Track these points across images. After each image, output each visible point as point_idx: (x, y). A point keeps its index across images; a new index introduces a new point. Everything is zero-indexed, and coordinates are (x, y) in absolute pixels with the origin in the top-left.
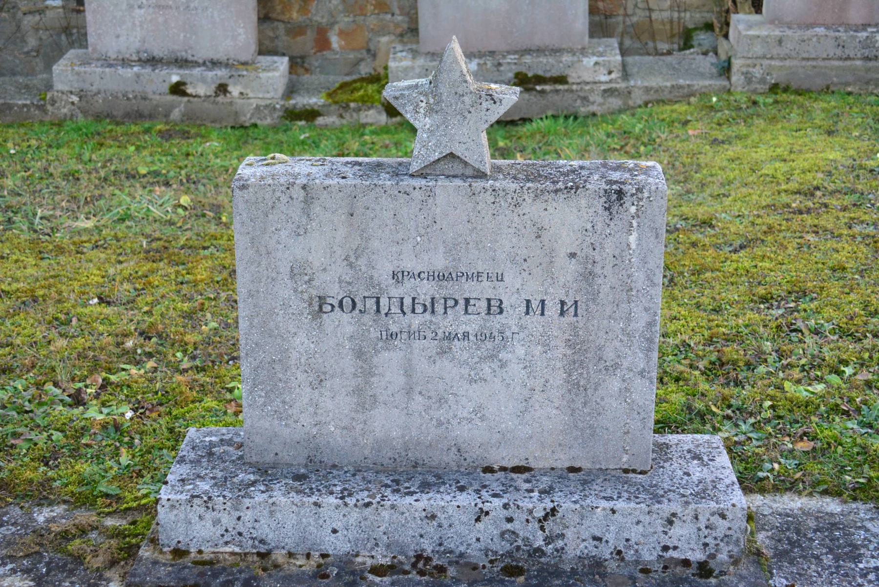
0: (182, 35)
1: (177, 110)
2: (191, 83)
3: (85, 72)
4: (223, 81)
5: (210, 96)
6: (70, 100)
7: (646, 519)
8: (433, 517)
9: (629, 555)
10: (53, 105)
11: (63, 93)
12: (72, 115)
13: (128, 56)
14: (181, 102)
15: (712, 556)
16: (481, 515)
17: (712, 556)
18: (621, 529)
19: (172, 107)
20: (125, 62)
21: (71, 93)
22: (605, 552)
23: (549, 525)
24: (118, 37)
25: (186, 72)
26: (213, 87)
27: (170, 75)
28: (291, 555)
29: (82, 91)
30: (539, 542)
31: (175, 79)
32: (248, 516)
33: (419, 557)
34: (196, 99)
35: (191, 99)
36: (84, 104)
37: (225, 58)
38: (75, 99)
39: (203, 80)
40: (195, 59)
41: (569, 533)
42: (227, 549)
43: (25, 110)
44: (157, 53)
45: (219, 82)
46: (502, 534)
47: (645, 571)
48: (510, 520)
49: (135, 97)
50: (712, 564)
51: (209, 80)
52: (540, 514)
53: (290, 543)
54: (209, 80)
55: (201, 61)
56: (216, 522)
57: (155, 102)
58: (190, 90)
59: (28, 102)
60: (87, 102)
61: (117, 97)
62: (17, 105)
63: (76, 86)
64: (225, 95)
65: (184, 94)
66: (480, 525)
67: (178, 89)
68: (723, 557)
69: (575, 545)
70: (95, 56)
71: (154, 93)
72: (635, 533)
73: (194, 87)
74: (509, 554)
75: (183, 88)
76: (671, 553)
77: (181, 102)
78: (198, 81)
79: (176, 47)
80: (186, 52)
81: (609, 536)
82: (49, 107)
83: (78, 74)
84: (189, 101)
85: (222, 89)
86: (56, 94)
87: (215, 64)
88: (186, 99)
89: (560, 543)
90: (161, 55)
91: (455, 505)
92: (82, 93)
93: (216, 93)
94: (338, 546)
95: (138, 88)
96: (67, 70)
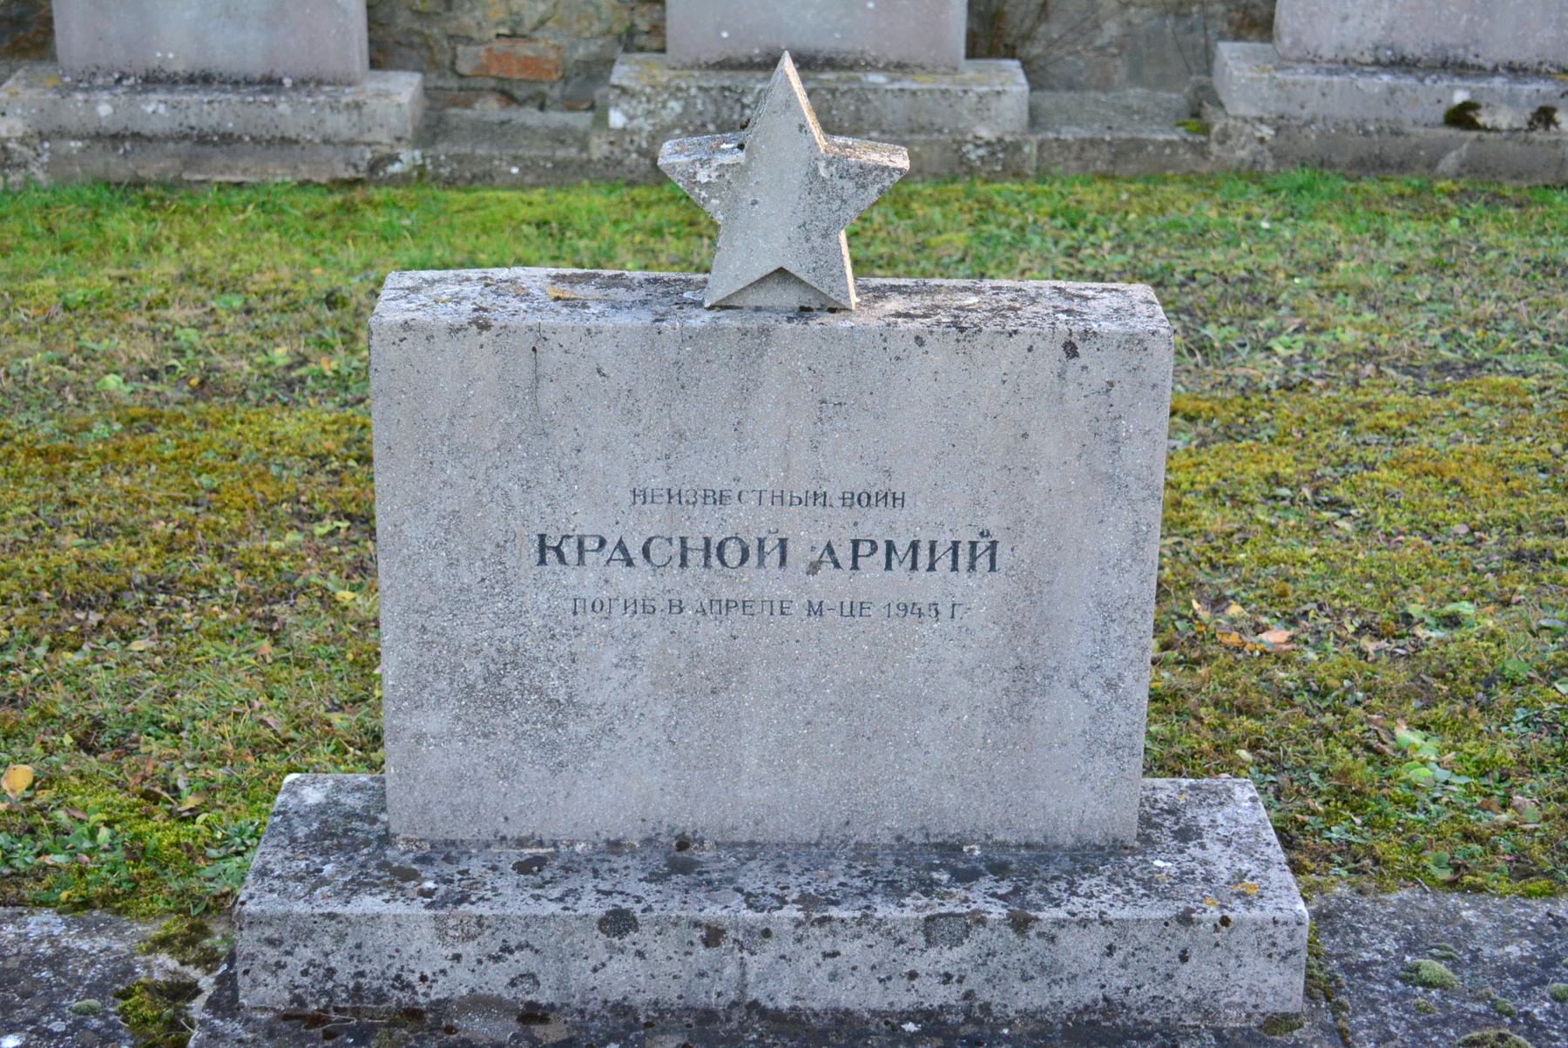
0: (1465, 17)
1: (1453, 154)
2: (1488, 105)
3: (1294, 84)
4: (1547, 103)
5: (1518, 130)
6: (1258, 134)
10: (1222, 143)
11: (1245, 121)
12: (1255, 162)
13: (1355, 55)
14: (1463, 141)
19: (1445, 148)
20: (1349, 65)
21: (1261, 120)
24: (1345, 19)
25: (1483, 85)
26: (1527, 113)
27: (1452, 89)
29: (1282, 117)
31: (1460, 97)
34: (1492, 135)
35: (1484, 135)
36: (1282, 141)
37: (1537, 60)
38: (1267, 132)
39: (1512, 100)
40: (1480, 61)
43: (1168, 151)
44: (1411, 49)
45: (1540, 103)
49: (1380, 131)
51: (1523, 99)
54: (1523, 99)
55: (1489, 66)
57: (1414, 140)
58: (1483, 119)
59: (1175, 137)
60: (1288, 138)
61: (1345, 130)
62: (1153, 142)
63: (1274, 108)
64: (1547, 128)
65: (1472, 125)
67: (1461, 117)
70: (1297, 53)
71: (1415, 123)
73: (1493, 113)
75: (1472, 114)
77: (1463, 141)
78: (1502, 101)
79: (1448, 40)
80: (1466, 48)
82: (1214, 148)
83: (1281, 86)
84: (1479, 139)
85: (1545, 116)
86: (1232, 122)
87: (1515, 71)
88: (1473, 134)
90: (1418, 53)
92: (1281, 122)
93: (1530, 123)
95: (1387, 113)
96: (1262, 79)
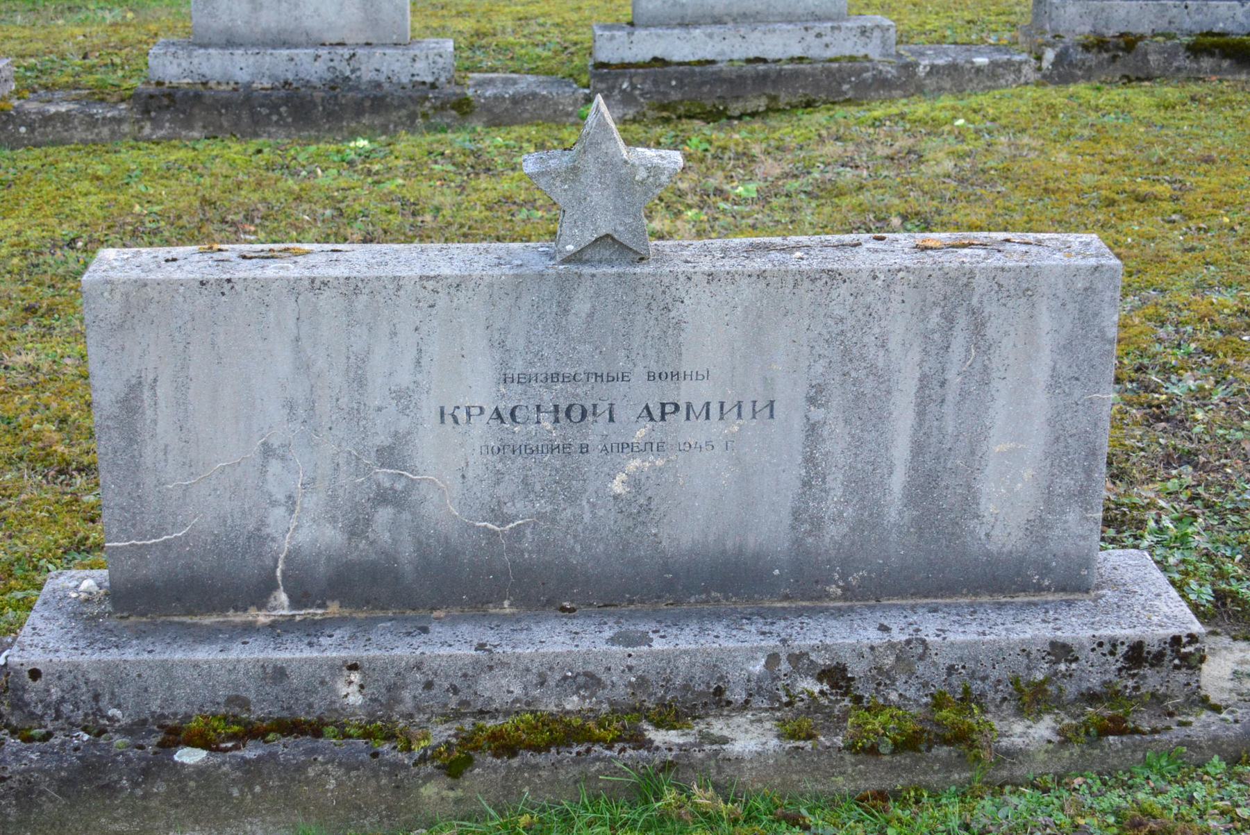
7: (401, 58)
8: (292, 60)
9: (395, 79)
15: (437, 79)
16: (317, 57)
17: (437, 79)
18: (389, 64)
22: (382, 78)
23: (352, 62)
28: (219, 83)
30: (348, 73)
32: (196, 61)
33: (286, 83)
41: (363, 68)
42: (186, 81)
46: (328, 69)
47: (403, 88)
48: (332, 60)
50: (437, 84)
52: (347, 56)
53: (218, 76)
56: (179, 65)
66: (317, 64)
68: (442, 79)
69: (367, 74)
72: (396, 67)
74: (332, 80)
76: (416, 78)
81: (384, 69)
89: (358, 73)
91: (304, 54)
94: (243, 77)
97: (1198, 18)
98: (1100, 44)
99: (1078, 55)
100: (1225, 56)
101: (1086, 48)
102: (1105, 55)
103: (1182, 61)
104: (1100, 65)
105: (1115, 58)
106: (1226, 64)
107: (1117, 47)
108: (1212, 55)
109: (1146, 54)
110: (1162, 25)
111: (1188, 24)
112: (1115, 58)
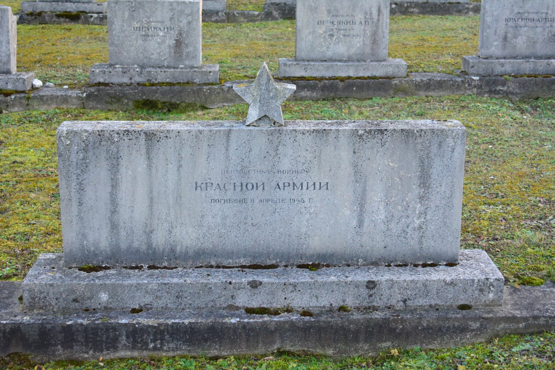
97: (62, 7)
98: (31, 14)
99: (26, 17)
100: (67, 18)
101: (28, 15)
102: (33, 17)
103: (55, 19)
104: (32, 20)
105: (36, 18)
106: (67, 20)
107: (36, 15)
108: (63, 17)
109: (44, 17)
110: (52, 9)
111: (59, 9)
112: (36, 18)
